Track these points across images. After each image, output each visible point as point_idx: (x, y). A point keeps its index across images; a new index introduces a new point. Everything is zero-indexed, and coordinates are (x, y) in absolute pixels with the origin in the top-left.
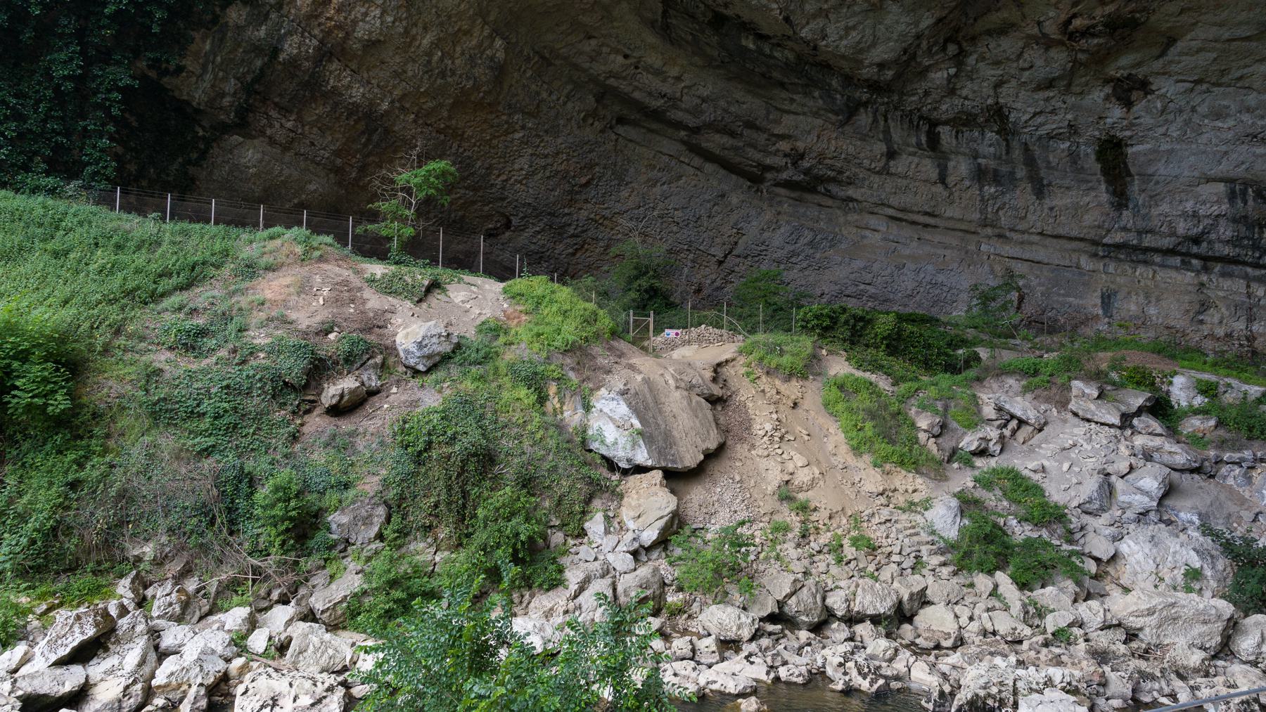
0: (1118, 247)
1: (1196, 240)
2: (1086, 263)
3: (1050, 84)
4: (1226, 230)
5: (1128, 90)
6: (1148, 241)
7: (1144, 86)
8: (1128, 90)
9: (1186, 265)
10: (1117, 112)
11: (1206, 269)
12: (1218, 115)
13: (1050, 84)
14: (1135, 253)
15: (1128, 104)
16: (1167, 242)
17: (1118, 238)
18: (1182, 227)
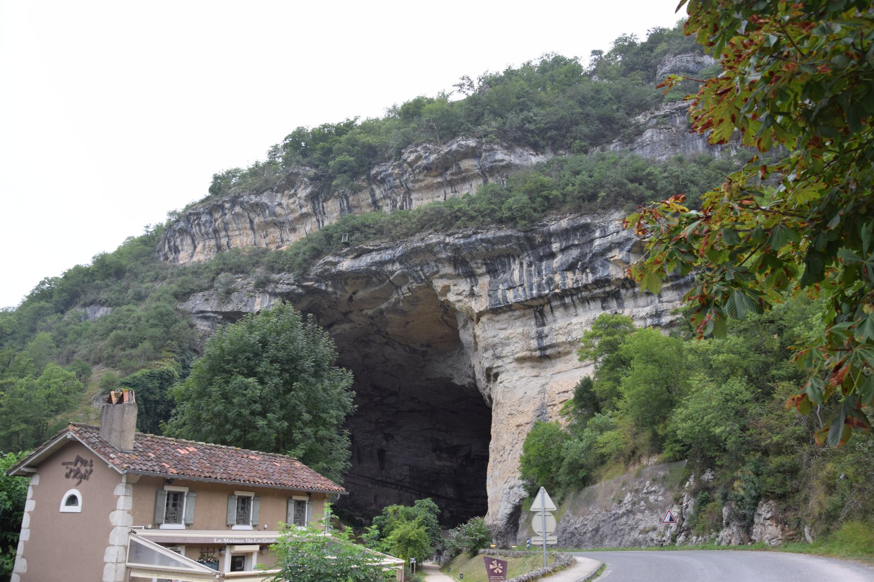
0: (378, 481)
1: (400, 481)
2: (370, 486)
3: (369, 432)
4: (408, 480)
5: (388, 437)
6: (388, 480)
7: (392, 437)
8: (388, 437)
9: (397, 488)
10: (385, 442)
11: (401, 489)
12: (409, 447)
13: (369, 432)
14: (384, 483)
15: (388, 441)
16: (393, 481)
17: (380, 478)
18: (398, 477)
